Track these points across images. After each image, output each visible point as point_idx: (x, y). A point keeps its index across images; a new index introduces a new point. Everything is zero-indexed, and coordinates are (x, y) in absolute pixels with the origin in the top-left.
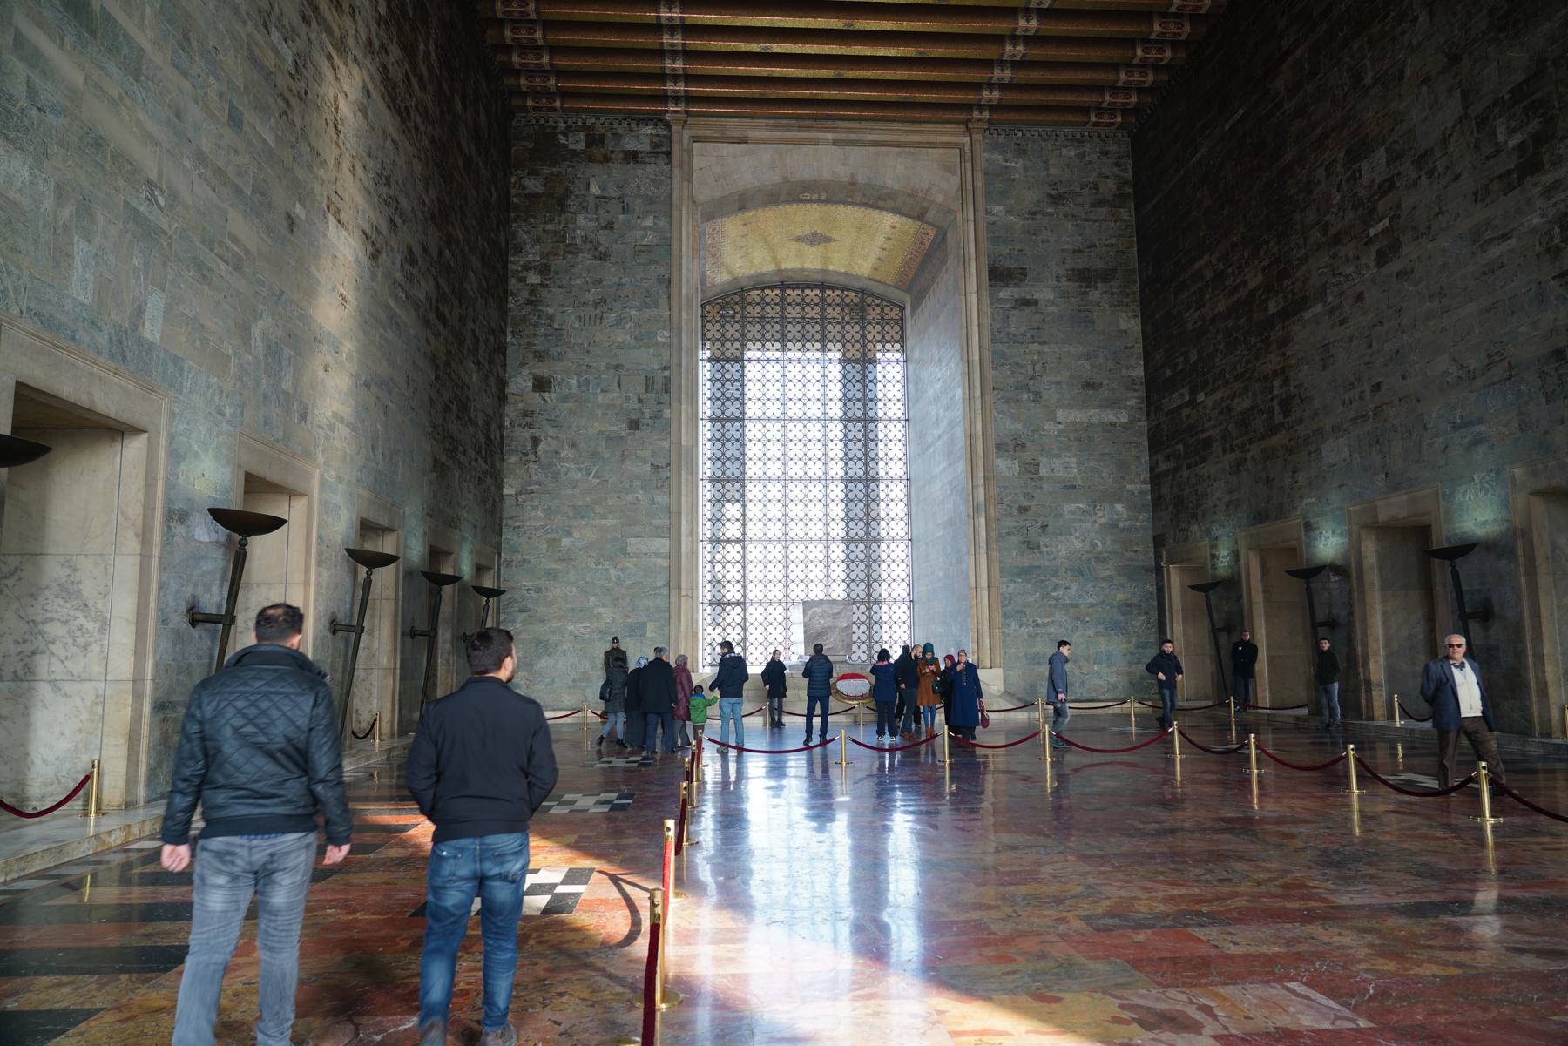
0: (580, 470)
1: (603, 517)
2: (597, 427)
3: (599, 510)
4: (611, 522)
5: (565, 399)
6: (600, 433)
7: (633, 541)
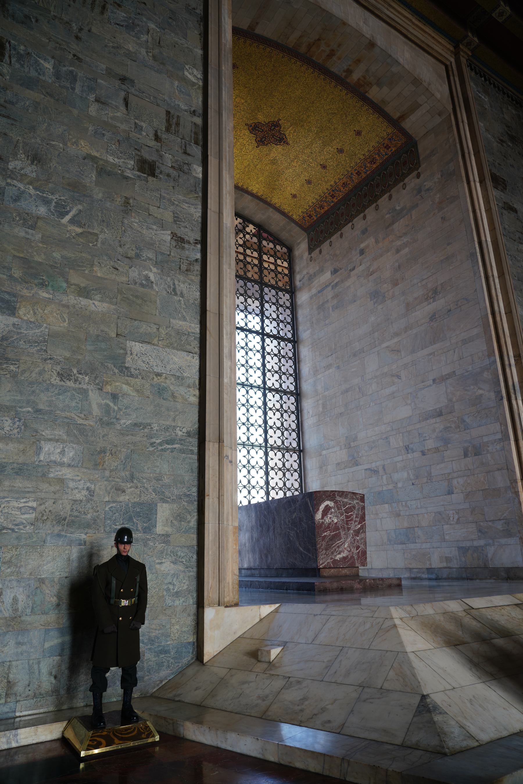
0: (46, 202)
1: (84, 292)
2: (84, 147)
3: (75, 278)
4: (97, 305)
5: (29, 83)
6: (88, 157)
7: (137, 347)
